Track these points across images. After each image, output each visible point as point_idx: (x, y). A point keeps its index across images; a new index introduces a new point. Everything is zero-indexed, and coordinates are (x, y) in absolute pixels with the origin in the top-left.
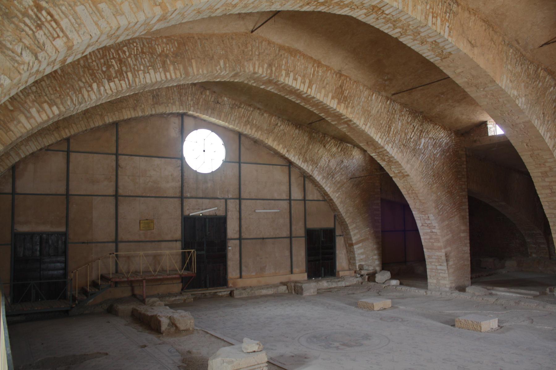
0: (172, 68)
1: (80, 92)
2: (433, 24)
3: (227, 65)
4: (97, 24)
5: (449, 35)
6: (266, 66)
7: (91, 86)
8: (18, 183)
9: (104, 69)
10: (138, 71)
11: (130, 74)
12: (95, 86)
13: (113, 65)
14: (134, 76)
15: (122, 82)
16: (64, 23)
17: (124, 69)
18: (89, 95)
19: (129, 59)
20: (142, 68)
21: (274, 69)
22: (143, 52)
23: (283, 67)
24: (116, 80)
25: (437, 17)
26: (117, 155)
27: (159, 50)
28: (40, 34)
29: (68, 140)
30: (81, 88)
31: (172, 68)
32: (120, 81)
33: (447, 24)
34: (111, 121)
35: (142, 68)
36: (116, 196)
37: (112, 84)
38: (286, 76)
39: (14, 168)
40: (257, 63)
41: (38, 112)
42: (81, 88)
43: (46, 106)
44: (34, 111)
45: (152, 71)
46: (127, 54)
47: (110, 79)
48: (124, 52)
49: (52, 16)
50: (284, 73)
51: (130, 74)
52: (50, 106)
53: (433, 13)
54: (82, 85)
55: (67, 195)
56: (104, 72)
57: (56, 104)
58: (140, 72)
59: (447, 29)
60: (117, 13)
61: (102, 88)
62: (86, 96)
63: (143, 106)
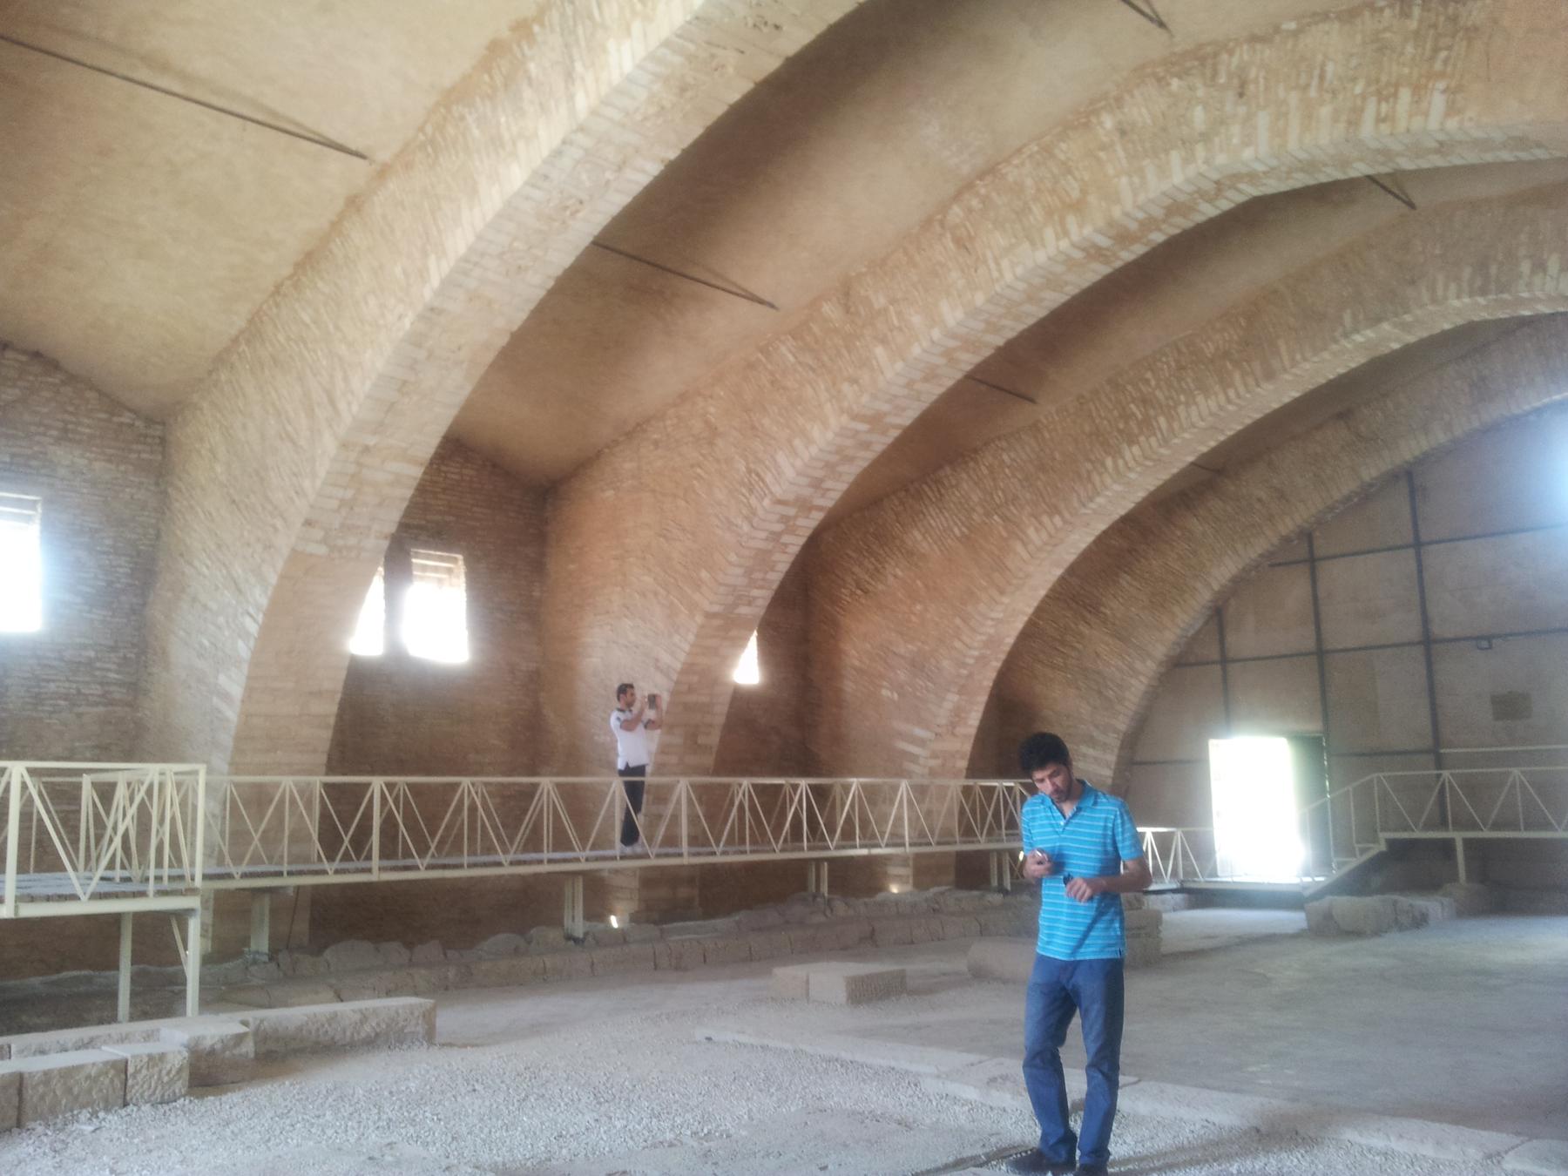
0: (1237, 377)
1: (1089, 478)
2: (1380, 120)
3: (1361, 317)
4: (793, 466)
5: (1451, 110)
6: (1467, 272)
7: (1103, 465)
8: (1231, 639)
9: (1121, 426)
10: (1175, 408)
11: (1162, 420)
12: (1109, 462)
13: (1134, 414)
14: (1170, 419)
15: (1153, 440)
16: (768, 478)
17: (1152, 412)
18: (1102, 482)
19: (1158, 393)
20: (1182, 398)
21: (1493, 270)
22: (1181, 368)
23: (1522, 252)
24: (1142, 439)
25: (1395, 95)
26: (1418, 545)
27: (1209, 349)
28: (753, 501)
29: (1307, 536)
30: (1089, 472)
31: (1237, 377)
32: (1147, 438)
33: (1441, 85)
34: (1374, 473)
35: (1182, 398)
36: (1428, 642)
37: (1135, 449)
38: (1533, 272)
39: (1218, 615)
40: (1441, 278)
41: (1037, 530)
42: (1089, 472)
43: (1045, 519)
44: (1031, 532)
45: (1200, 399)
46: (1153, 383)
47: (1132, 441)
48: (1147, 381)
49: (758, 475)
50: (1525, 267)
51: (1162, 420)
52: (1051, 516)
53: (1379, 93)
54: (1089, 466)
55: (1321, 654)
56: (1120, 431)
57: (1060, 513)
58: (1181, 409)
59: (1438, 102)
60: (809, 441)
61: (1121, 462)
62: (1098, 483)
63: (1447, 417)
